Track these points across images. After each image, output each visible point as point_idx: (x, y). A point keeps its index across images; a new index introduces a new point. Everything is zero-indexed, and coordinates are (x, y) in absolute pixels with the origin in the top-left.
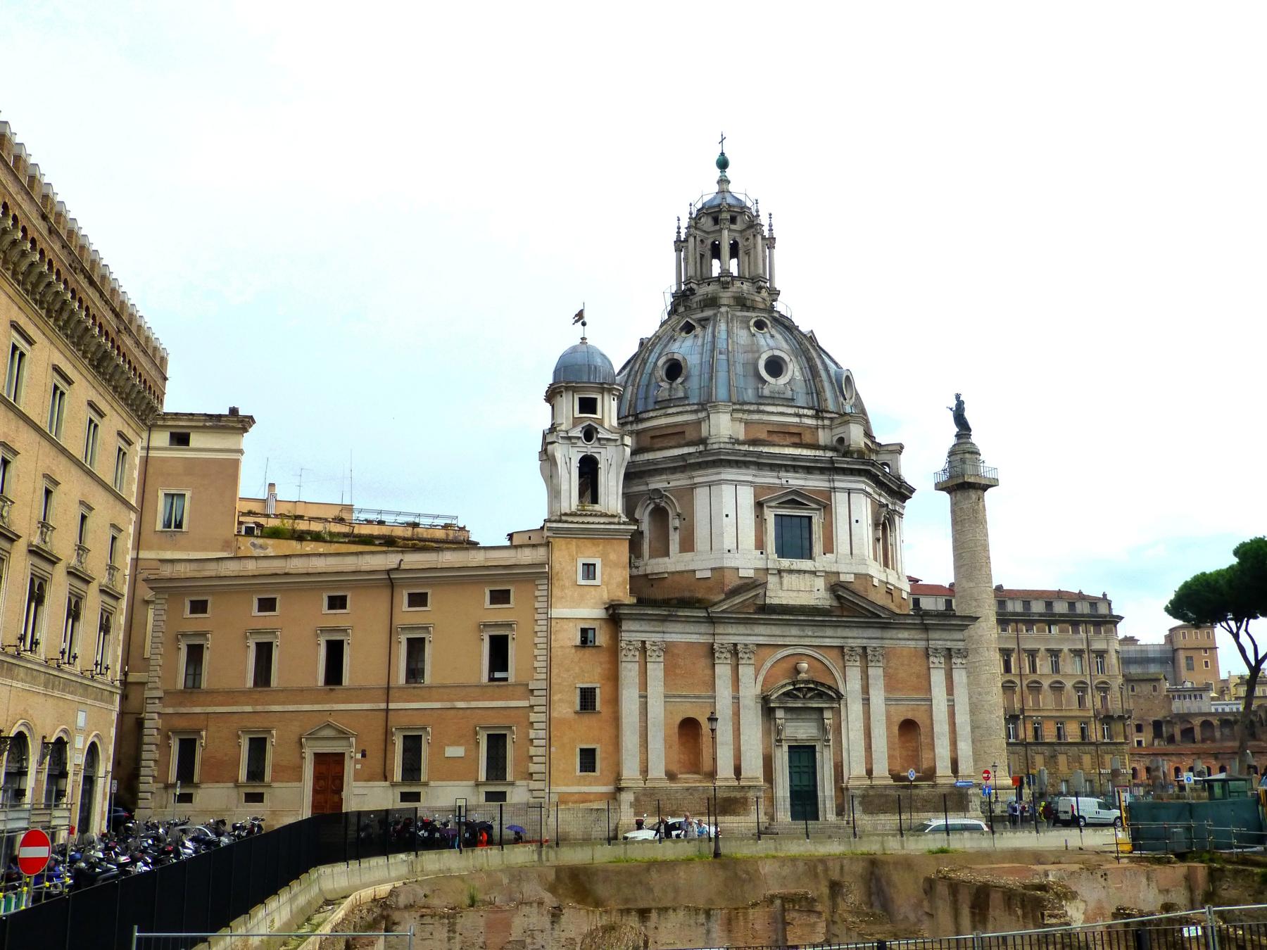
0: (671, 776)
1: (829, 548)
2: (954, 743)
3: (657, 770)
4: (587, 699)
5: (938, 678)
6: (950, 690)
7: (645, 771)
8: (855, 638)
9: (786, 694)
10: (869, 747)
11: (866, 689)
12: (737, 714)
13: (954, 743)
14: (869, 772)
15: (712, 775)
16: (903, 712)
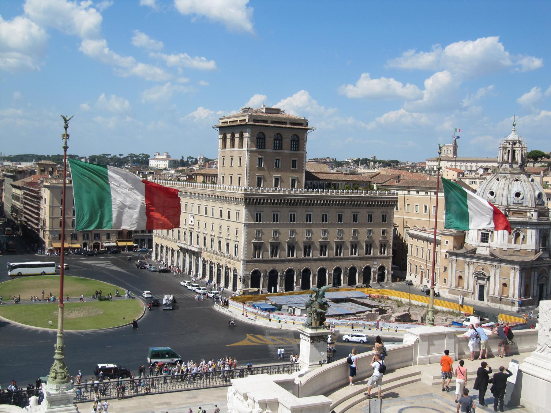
0: (456, 287)
1: (492, 241)
2: (514, 290)
3: (454, 286)
4: (445, 268)
5: (512, 274)
6: (514, 277)
7: (451, 285)
8: (494, 264)
9: (477, 274)
10: (495, 288)
11: (495, 275)
12: (468, 276)
13: (514, 290)
14: (494, 293)
15: (463, 288)
16: (503, 281)
